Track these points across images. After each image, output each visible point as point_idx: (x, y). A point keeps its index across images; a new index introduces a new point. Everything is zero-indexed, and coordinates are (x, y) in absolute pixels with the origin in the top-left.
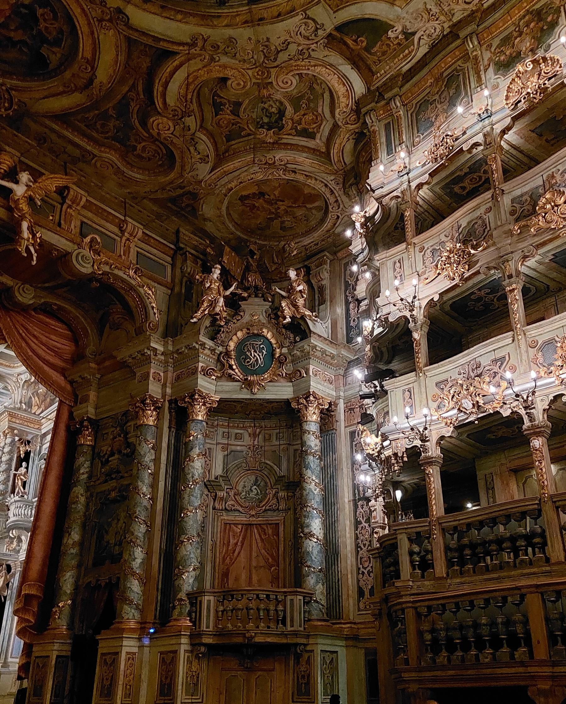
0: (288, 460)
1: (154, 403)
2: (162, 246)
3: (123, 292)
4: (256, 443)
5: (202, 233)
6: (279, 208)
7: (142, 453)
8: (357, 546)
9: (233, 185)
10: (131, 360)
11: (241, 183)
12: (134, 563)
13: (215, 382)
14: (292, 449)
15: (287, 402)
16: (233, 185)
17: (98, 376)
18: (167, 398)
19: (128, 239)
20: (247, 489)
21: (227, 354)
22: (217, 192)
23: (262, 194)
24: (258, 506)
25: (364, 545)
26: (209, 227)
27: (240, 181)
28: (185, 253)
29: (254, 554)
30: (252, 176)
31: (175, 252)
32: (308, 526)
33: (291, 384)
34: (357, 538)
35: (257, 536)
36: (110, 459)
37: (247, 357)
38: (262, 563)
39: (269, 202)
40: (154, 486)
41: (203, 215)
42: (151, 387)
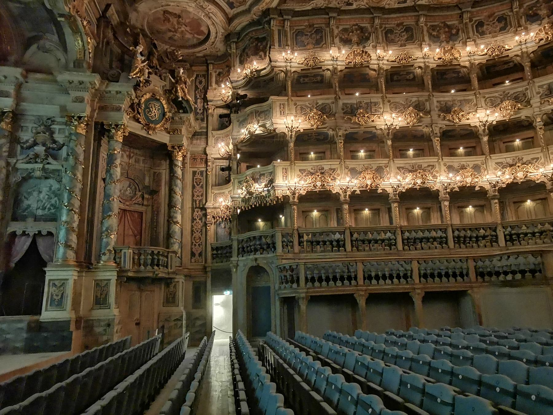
0: (150, 177)
5: (125, 16)
8: (192, 231)
9: (172, 4)
14: (152, 171)
15: (164, 145)
16: (172, 4)
23: (179, 17)
25: (197, 231)
29: (126, 228)
31: (100, 17)
32: (176, 218)
33: (169, 135)
34: (192, 227)
35: (129, 217)
37: (150, 111)
38: (131, 233)
39: (178, 23)
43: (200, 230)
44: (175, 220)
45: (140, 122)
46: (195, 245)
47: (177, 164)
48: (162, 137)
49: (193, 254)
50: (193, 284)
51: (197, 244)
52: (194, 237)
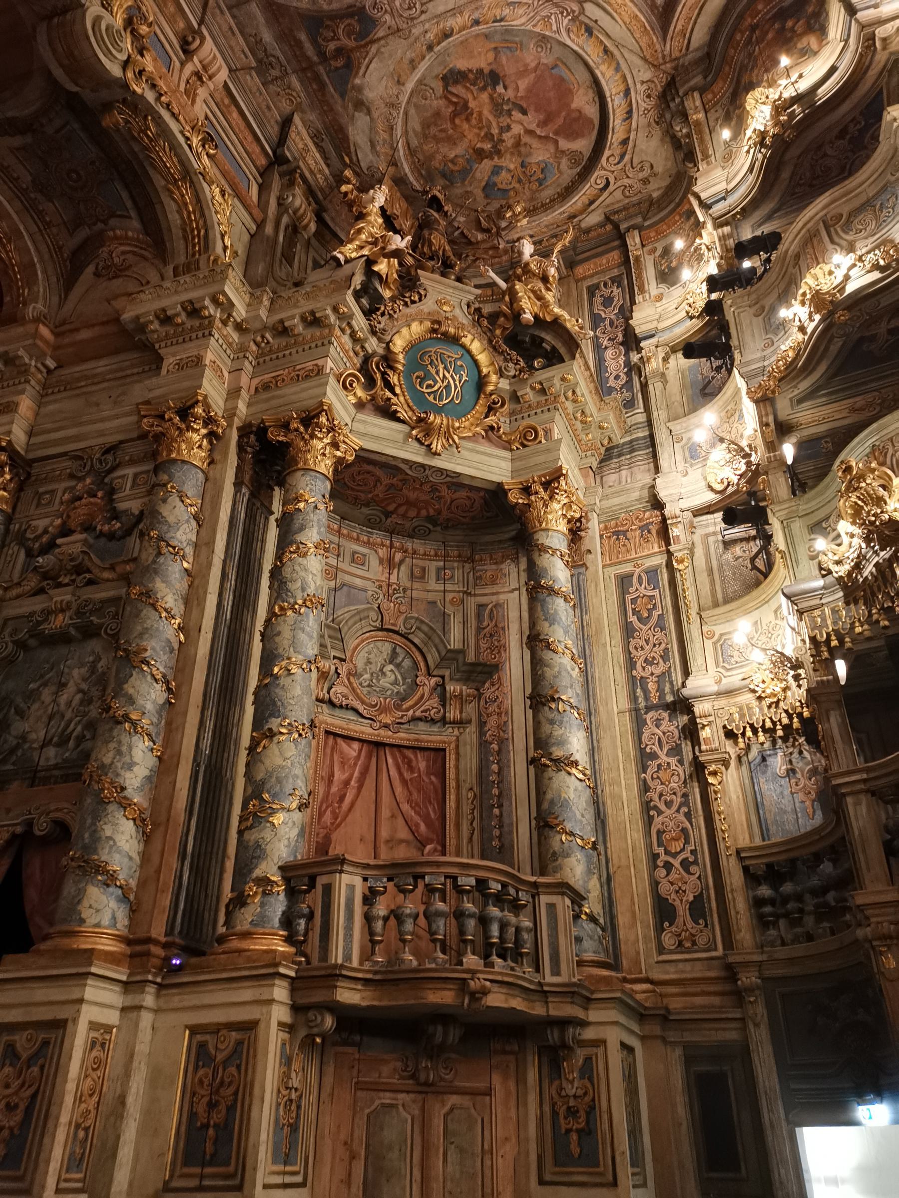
0: (464, 623)
1: (209, 421)
2: (250, 138)
3: (159, 182)
4: (393, 579)
6: (509, 128)
7: (171, 519)
8: (647, 807)
9: (455, 22)
10: (155, 326)
11: (477, 22)
12: (128, 775)
13: (353, 410)
14: (471, 603)
15: (498, 492)
16: (455, 22)
17: (51, 364)
18: (237, 422)
19: (197, 74)
20: (375, 668)
21: (388, 359)
22: (416, 31)
23: (494, 78)
24: (398, 707)
25: (668, 804)
26: (358, 131)
27: (476, 15)
28: (294, 171)
29: (385, 813)
30: (506, 11)
31: (271, 165)
32: (562, 743)
33: (507, 454)
34: (645, 788)
35: (393, 772)
36: (59, 541)
37: (427, 376)
38: (403, 833)
39: (498, 107)
40: (192, 599)
41: (359, 89)
42: (205, 382)
43: (678, 800)
44: (557, 753)
45: (393, 416)
46: (668, 866)
47: (547, 542)
48: (486, 464)
49: (664, 911)
50: (689, 1060)
51: (676, 863)
52: (660, 833)
